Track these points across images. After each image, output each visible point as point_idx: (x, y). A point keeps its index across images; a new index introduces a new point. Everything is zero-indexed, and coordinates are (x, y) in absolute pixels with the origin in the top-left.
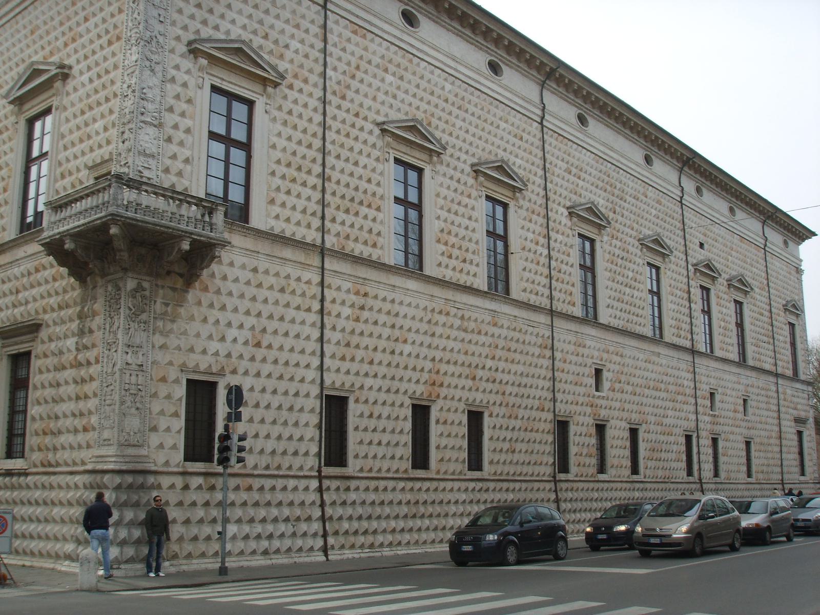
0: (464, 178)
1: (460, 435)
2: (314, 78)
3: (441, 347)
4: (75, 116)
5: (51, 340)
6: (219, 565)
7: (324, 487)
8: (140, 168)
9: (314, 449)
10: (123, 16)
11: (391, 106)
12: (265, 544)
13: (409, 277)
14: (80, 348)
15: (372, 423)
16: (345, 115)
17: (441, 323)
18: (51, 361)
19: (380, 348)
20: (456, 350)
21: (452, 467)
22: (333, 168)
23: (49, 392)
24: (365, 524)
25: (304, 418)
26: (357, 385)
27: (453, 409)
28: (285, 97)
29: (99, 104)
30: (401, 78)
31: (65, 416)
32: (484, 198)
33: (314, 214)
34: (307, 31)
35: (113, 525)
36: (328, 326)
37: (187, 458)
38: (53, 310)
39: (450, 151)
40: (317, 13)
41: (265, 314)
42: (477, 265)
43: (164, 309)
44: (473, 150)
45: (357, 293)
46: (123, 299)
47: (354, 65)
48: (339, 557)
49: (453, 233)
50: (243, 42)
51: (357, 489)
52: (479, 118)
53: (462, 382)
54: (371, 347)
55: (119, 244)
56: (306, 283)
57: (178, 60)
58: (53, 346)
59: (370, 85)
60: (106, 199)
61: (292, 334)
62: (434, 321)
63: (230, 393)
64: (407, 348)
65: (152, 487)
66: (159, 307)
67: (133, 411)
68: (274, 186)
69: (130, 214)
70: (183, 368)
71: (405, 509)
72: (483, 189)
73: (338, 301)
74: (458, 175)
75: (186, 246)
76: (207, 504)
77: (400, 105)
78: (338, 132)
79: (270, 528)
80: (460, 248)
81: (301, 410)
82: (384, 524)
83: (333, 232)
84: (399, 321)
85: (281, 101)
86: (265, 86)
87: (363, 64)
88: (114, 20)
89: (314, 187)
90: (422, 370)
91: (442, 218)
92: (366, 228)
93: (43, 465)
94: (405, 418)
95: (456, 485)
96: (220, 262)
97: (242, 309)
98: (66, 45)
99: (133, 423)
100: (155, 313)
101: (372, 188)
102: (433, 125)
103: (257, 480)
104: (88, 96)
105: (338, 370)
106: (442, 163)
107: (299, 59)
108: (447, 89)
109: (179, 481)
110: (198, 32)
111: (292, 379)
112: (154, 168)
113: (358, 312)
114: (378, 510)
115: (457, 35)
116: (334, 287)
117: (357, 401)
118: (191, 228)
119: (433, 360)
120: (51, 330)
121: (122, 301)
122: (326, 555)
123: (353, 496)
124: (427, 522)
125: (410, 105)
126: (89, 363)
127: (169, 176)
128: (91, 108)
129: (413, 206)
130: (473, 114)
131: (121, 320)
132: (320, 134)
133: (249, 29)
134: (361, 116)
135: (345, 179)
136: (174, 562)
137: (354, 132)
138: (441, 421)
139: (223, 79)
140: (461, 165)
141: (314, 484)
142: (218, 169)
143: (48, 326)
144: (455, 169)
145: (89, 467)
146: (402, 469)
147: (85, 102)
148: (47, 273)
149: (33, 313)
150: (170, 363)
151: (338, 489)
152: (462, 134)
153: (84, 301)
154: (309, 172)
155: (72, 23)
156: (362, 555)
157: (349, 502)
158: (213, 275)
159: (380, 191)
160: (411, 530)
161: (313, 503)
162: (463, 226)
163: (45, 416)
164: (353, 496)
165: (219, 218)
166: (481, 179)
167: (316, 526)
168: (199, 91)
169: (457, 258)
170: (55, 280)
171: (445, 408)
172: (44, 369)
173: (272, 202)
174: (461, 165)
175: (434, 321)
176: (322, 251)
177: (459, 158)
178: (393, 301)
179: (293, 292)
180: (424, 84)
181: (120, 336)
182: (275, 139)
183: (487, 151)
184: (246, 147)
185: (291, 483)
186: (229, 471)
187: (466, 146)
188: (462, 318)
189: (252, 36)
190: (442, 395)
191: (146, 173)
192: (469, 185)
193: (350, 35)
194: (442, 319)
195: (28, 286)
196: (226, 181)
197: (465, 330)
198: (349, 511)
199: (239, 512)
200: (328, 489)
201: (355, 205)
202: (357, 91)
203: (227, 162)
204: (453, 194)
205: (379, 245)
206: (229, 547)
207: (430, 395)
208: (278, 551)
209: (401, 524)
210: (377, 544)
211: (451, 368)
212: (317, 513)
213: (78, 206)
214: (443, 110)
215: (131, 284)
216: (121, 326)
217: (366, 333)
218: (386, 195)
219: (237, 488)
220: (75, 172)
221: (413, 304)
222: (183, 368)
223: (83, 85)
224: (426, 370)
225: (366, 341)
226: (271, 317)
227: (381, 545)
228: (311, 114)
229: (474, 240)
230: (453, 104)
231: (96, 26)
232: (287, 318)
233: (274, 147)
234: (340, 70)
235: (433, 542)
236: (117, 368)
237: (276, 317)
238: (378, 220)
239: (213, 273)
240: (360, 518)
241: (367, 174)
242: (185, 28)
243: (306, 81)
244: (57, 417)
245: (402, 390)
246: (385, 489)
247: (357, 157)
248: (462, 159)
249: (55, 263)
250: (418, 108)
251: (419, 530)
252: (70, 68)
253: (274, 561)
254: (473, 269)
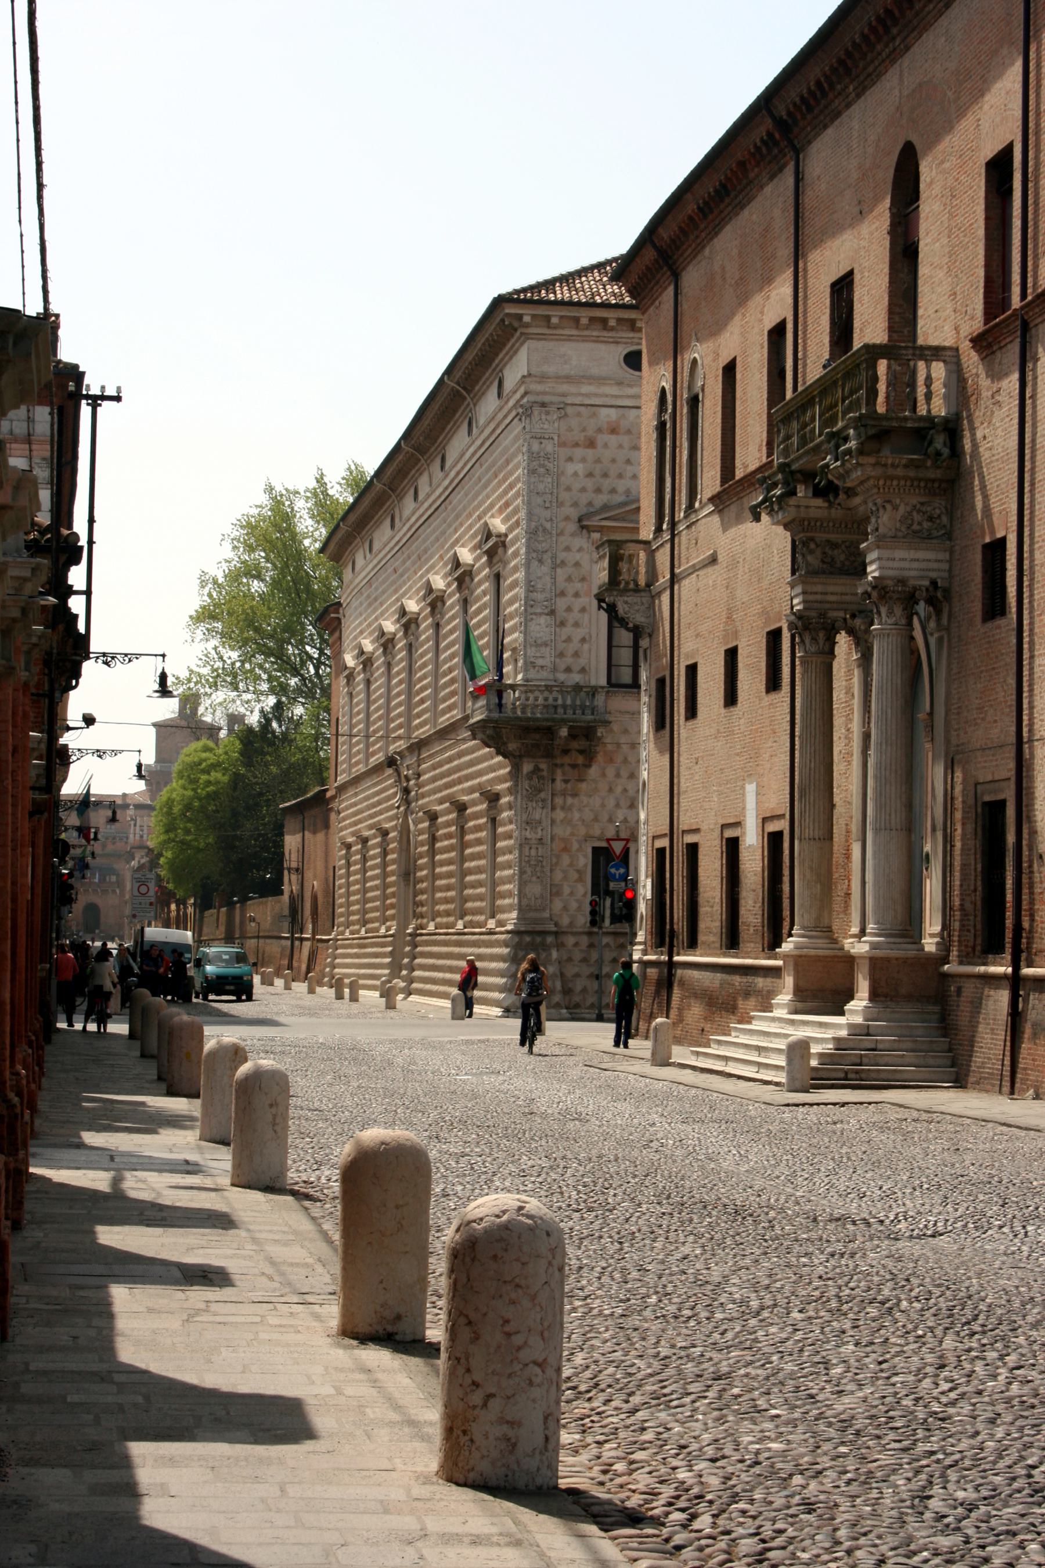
43: (564, 786)
66: (559, 785)
150: (572, 834)
242: (575, 504)
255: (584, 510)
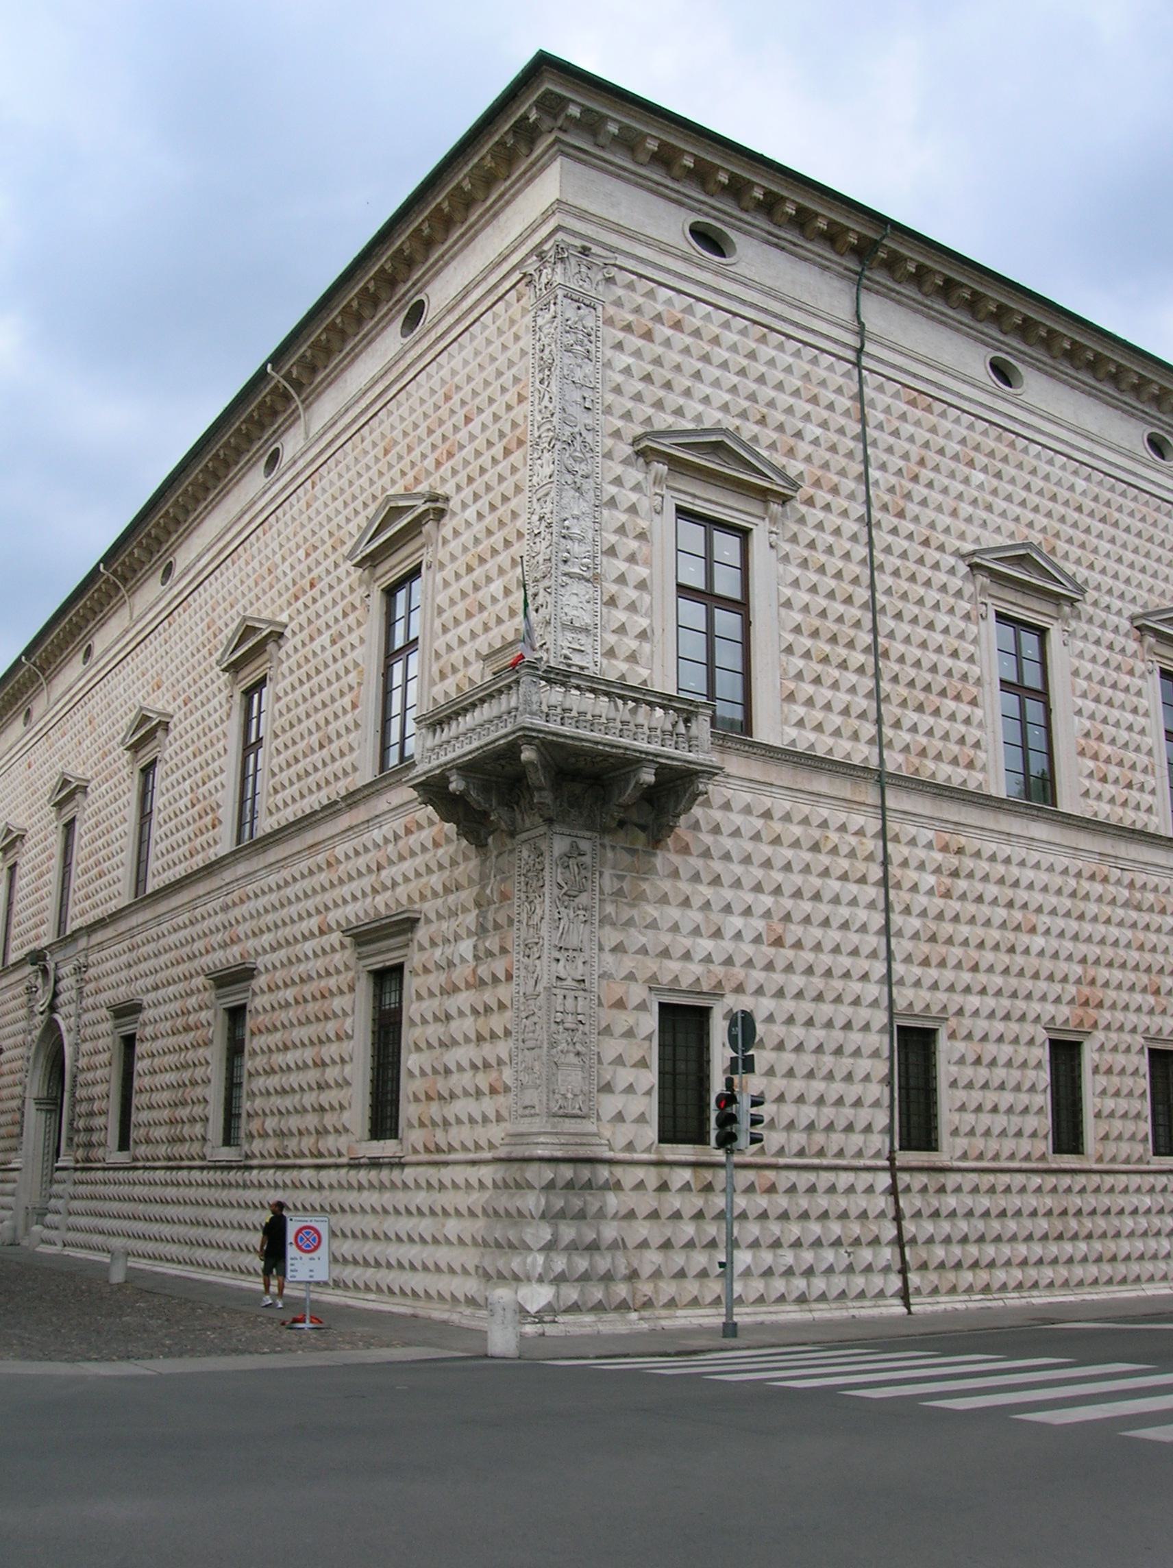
0: (1120, 641)
1: (1137, 1092)
2: (849, 485)
3: (1097, 938)
4: (458, 576)
5: (433, 944)
6: (723, 1319)
7: (901, 1186)
8: (566, 652)
9: (882, 1119)
10: (526, 406)
11: (984, 524)
12: (800, 1284)
13: (1036, 818)
14: (481, 954)
15: (983, 1073)
16: (906, 544)
17: (1093, 896)
18: (435, 980)
19: (989, 943)
20: (1123, 942)
21: (1125, 1148)
22: (891, 635)
23: (434, 1031)
24: (973, 1250)
25: (864, 1065)
26: (953, 1009)
27: (1123, 1047)
28: (802, 520)
29: (494, 552)
30: (998, 475)
31: (460, 1068)
32: (1157, 674)
33: (863, 716)
34: (831, 407)
35: (541, 1249)
36: (898, 908)
37: (662, 1139)
38: (435, 894)
39: (1091, 595)
40: (847, 375)
41: (788, 890)
42: (1153, 792)
44: (1132, 591)
45: (945, 849)
46: (547, 869)
47: (915, 458)
48: (929, 1308)
49: (1107, 739)
50: (725, 432)
51: (958, 1189)
52: (1139, 534)
53: (1138, 998)
54: (974, 942)
55: (537, 778)
56: (856, 834)
57: (619, 469)
58: (438, 952)
59: (945, 491)
60: (513, 704)
61: (835, 923)
62: (1081, 893)
63: (733, 1024)
64: (1038, 942)
65: (606, 1187)
66: (608, 883)
67: (572, 1058)
68: (792, 672)
69: (553, 726)
70: (653, 984)
71: (1043, 1224)
72: (1155, 658)
73: (913, 863)
74: (1109, 636)
75: (648, 777)
76: (699, 1215)
77: (999, 521)
78: (896, 573)
79: (808, 1256)
80: (1120, 764)
81: (857, 1053)
82: (1006, 1250)
83: (898, 745)
84: (1022, 895)
85: (795, 527)
86: (766, 502)
87: (932, 457)
88: (512, 414)
89: (861, 670)
90: (1065, 979)
91: (1086, 713)
92: (954, 736)
93: (427, 1150)
94: (1039, 1065)
95: (1136, 1180)
96: (707, 804)
97: (748, 883)
98: (438, 464)
99: (572, 1079)
100: (602, 892)
101: (961, 666)
102: (1060, 553)
103: (784, 1173)
104: (477, 541)
105: (918, 984)
106: (1079, 617)
107: (823, 454)
108: (1079, 490)
109: (651, 1177)
110: (648, 420)
111: (838, 999)
112: (589, 650)
113: (948, 881)
114: (996, 1226)
115: (1090, 394)
116: (904, 839)
117: (952, 1036)
118: (654, 747)
119: (1083, 961)
120: (433, 927)
121: (546, 873)
122: (907, 1305)
123: (951, 1201)
124: (1083, 1246)
125: (1017, 519)
126: (495, 979)
127: (614, 662)
128: (482, 561)
129: (1030, 694)
130: (1127, 530)
131: (545, 906)
132: (865, 580)
133: (735, 410)
134: (934, 544)
135: (914, 652)
136: (645, 1313)
137: (926, 572)
138: (1103, 1068)
139: (694, 496)
140: (1113, 619)
141: (884, 1180)
142: (695, 646)
143: (428, 921)
144: (1103, 626)
145: (502, 1153)
146: (1036, 1154)
147: (473, 551)
148: (426, 835)
149: (404, 901)
150: (631, 977)
151: (924, 1189)
152: (1112, 566)
153: (483, 878)
154: (851, 644)
155: (447, 428)
156: (971, 1305)
157: (944, 1212)
158: (696, 826)
159: (975, 671)
160: (1055, 1261)
161: (882, 1214)
162: (1124, 725)
163: (429, 1070)
164: (951, 1201)
165: (701, 728)
166: (1150, 640)
167: (888, 1254)
168: (657, 518)
169: (1116, 781)
170: (436, 845)
171: (1108, 1046)
172: (424, 993)
173: (791, 698)
174: (1113, 619)
175: (1081, 893)
176: (881, 778)
177: (1108, 607)
178: (1008, 861)
179: (834, 851)
180: (1038, 483)
181: (544, 932)
182: (788, 592)
183: (1158, 591)
184: (742, 606)
185: (844, 1179)
186: (736, 1158)
187: (1120, 586)
188: (1132, 885)
189: (738, 422)
190: (1102, 1023)
191: (576, 659)
192: (1129, 652)
193: (905, 407)
194: (1097, 888)
195: (394, 858)
196: (710, 665)
197: (1138, 908)
198: (946, 1227)
199: (753, 1229)
200: (908, 1189)
201: (933, 697)
202: (924, 503)
203: (710, 634)
204: (1102, 671)
205: (978, 764)
206: (738, 1288)
207: (1081, 1023)
208: (823, 1297)
209: (1037, 1250)
210: (996, 1286)
211: (1117, 975)
212: (890, 1231)
213: (469, 720)
214: (1075, 525)
215: (560, 845)
216: (547, 917)
217: (964, 917)
218: (986, 678)
219: (750, 1189)
220: (461, 667)
221: (1044, 866)
222: (653, 984)
223: (468, 524)
224: (1072, 979)
225: (965, 930)
226: (798, 894)
227: (1004, 1287)
228: (848, 545)
229: (1145, 749)
230: (1091, 514)
231: (484, 427)
232: (827, 896)
233: (788, 604)
234: (892, 468)
235: (1095, 1282)
236: (540, 988)
237: (807, 894)
238: (975, 721)
239: (697, 821)
240: (964, 1240)
241: (952, 642)
242: (627, 416)
243: (835, 490)
244: (448, 1071)
245: (1031, 1016)
246: (1008, 1190)
247: (932, 615)
248: (1114, 609)
249: (436, 818)
250: (1030, 525)
251: (1070, 1260)
252: (447, 499)
253: (817, 1315)
254: (1147, 799)
255: (639, 430)
